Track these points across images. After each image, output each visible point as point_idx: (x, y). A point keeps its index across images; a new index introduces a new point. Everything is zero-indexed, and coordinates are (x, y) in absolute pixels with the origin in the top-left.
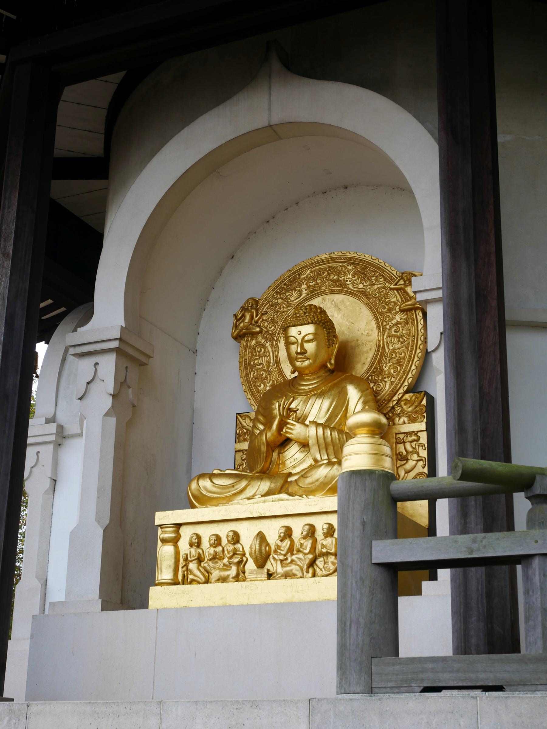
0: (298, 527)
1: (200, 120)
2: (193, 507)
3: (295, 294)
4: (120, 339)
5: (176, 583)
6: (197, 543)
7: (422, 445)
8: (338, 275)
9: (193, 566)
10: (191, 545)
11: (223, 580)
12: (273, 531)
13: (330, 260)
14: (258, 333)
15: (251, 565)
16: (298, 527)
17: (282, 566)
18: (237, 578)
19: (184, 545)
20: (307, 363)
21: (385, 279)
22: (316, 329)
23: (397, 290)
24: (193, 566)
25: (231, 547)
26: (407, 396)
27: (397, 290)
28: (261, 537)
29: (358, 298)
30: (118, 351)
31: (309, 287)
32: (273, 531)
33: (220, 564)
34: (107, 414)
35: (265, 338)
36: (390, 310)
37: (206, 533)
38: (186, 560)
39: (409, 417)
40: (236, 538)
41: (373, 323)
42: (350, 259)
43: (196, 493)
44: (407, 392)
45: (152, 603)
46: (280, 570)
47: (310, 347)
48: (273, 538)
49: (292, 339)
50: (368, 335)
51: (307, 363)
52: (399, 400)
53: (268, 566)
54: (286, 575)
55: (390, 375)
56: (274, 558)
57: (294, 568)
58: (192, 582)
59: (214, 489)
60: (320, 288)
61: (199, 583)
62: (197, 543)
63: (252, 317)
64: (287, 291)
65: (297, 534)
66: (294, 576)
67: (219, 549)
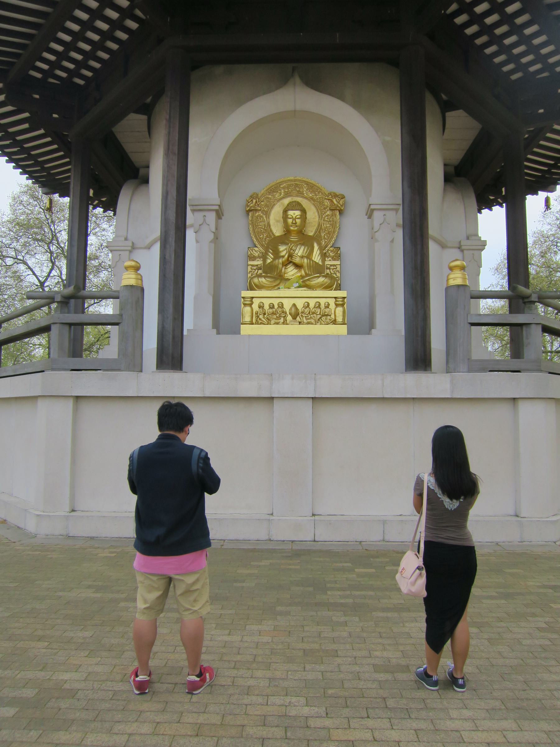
0: (312, 303)
1: (257, 99)
2: (255, 290)
3: (278, 194)
4: (219, 206)
5: (253, 324)
6: (261, 306)
7: (338, 271)
8: (299, 188)
9: (261, 317)
10: (260, 307)
11: (278, 323)
12: (300, 304)
13: (295, 180)
14: (260, 210)
15: (289, 318)
16: (312, 303)
17: (307, 319)
18: (283, 323)
19: (255, 307)
20: (296, 228)
21: (322, 194)
22: (301, 213)
23: (328, 199)
24: (261, 317)
25: (280, 310)
26: (331, 249)
27: (328, 199)
28: (294, 305)
29: (309, 200)
30: (217, 211)
31: (285, 191)
32: (300, 304)
33: (275, 317)
34: (211, 242)
35: (263, 213)
36: (325, 209)
37: (267, 302)
38: (257, 313)
39: (332, 258)
40: (281, 306)
41: (317, 214)
42: (305, 181)
43: (257, 283)
44: (331, 247)
45: (242, 332)
46: (305, 321)
47: (298, 221)
48: (300, 306)
49: (290, 216)
50: (314, 218)
51: (296, 228)
52: (328, 250)
53: (298, 319)
54: (308, 323)
55: (325, 238)
56: (302, 316)
57: (313, 321)
58: (261, 324)
59: (266, 283)
60: (290, 193)
61: (264, 324)
62: (261, 306)
63: (256, 202)
64: (274, 192)
65: (312, 305)
66: (312, 324)
67: (274, 310)
